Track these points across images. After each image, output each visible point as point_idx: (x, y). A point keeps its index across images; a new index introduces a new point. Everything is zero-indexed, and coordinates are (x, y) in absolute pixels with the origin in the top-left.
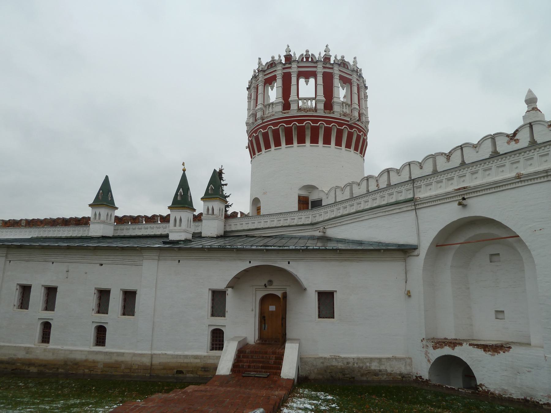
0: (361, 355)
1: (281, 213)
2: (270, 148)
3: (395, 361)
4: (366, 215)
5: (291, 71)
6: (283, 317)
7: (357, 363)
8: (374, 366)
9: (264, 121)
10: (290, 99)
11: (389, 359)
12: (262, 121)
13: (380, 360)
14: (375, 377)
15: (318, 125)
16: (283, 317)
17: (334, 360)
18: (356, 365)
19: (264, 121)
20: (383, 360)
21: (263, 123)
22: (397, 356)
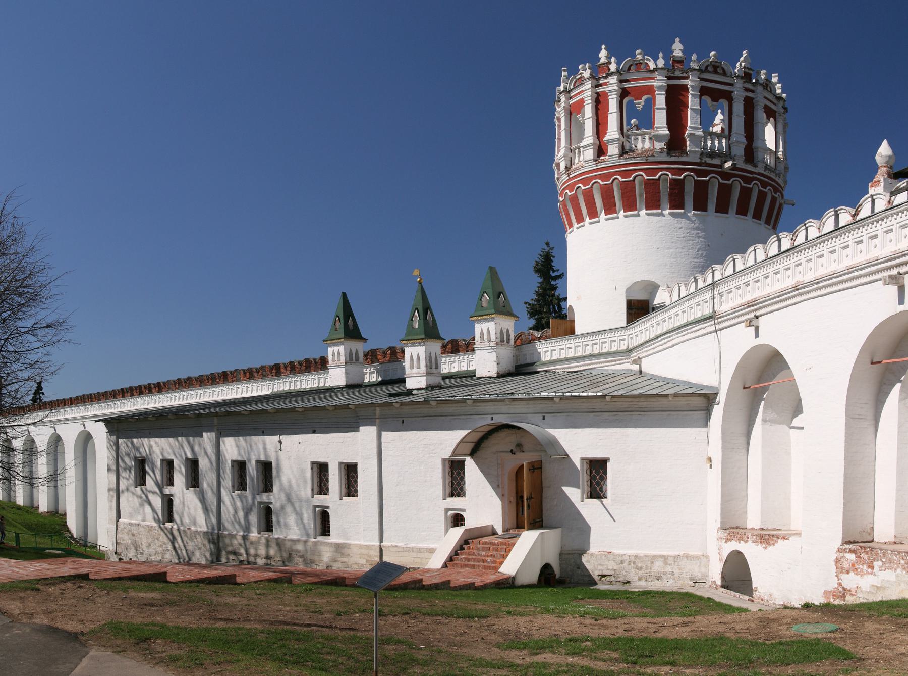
0: (642, 552)
1: (587, 334)
2: (583, 220)
3: (685, 559)
4: (677, 338)
5: (606, 90)
6: (531, 494)
7: (634, 563)
8: (658, 566)
9: (571, 176)
10: (606, 138)
11: (676, 558)
12: (568, 176)
13: (665, 558)
14: (657, 581)
15: (657, 177)
16: (531, 494)
17: (604, 557)
18: (632, 565)
19: (571, 176)
20: (669, 558)
21: (570, 179)
22: (690, 553)
